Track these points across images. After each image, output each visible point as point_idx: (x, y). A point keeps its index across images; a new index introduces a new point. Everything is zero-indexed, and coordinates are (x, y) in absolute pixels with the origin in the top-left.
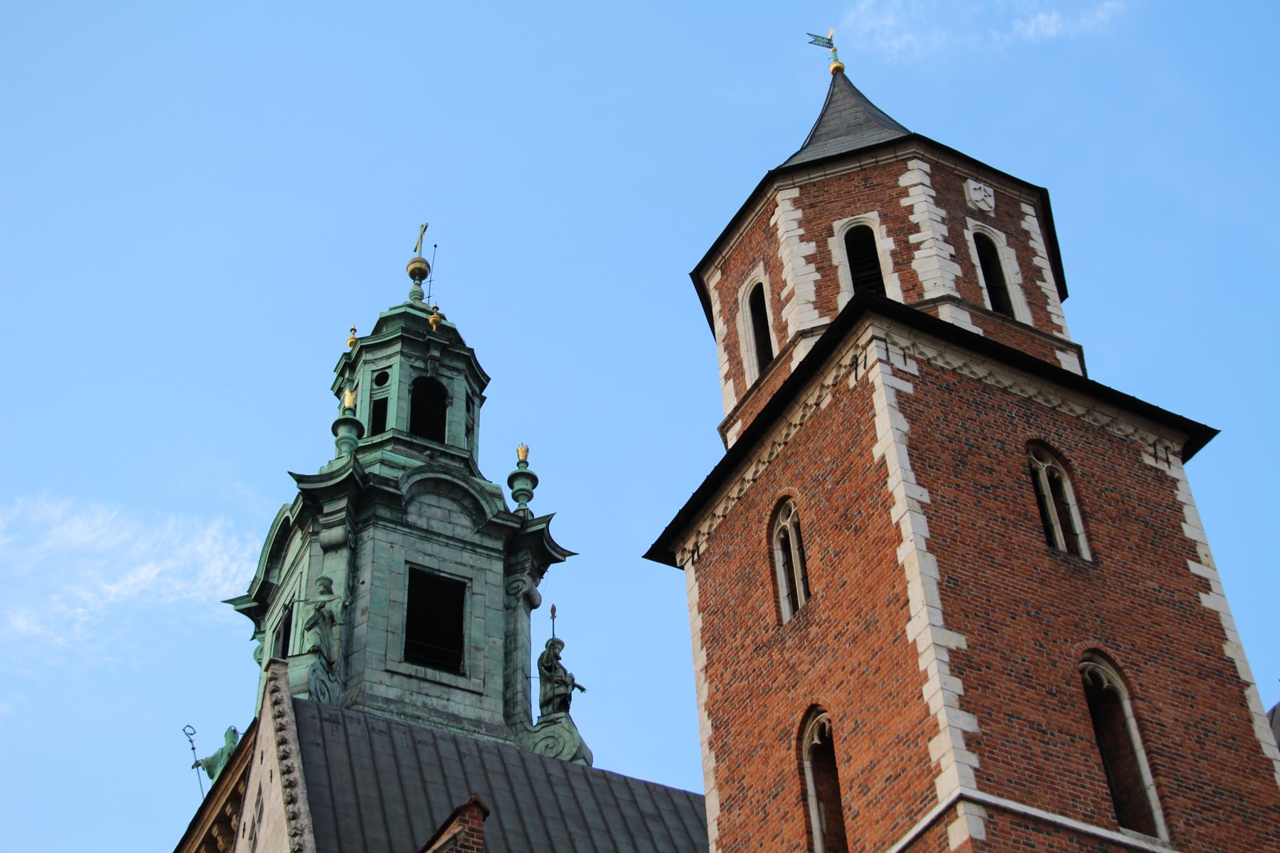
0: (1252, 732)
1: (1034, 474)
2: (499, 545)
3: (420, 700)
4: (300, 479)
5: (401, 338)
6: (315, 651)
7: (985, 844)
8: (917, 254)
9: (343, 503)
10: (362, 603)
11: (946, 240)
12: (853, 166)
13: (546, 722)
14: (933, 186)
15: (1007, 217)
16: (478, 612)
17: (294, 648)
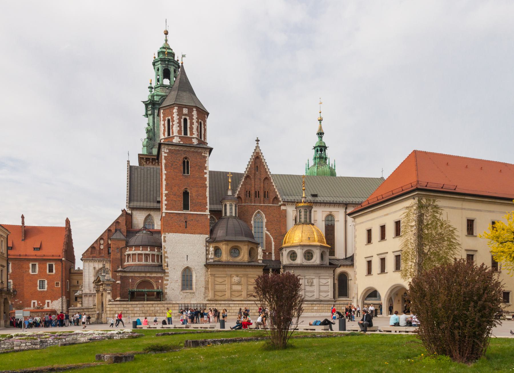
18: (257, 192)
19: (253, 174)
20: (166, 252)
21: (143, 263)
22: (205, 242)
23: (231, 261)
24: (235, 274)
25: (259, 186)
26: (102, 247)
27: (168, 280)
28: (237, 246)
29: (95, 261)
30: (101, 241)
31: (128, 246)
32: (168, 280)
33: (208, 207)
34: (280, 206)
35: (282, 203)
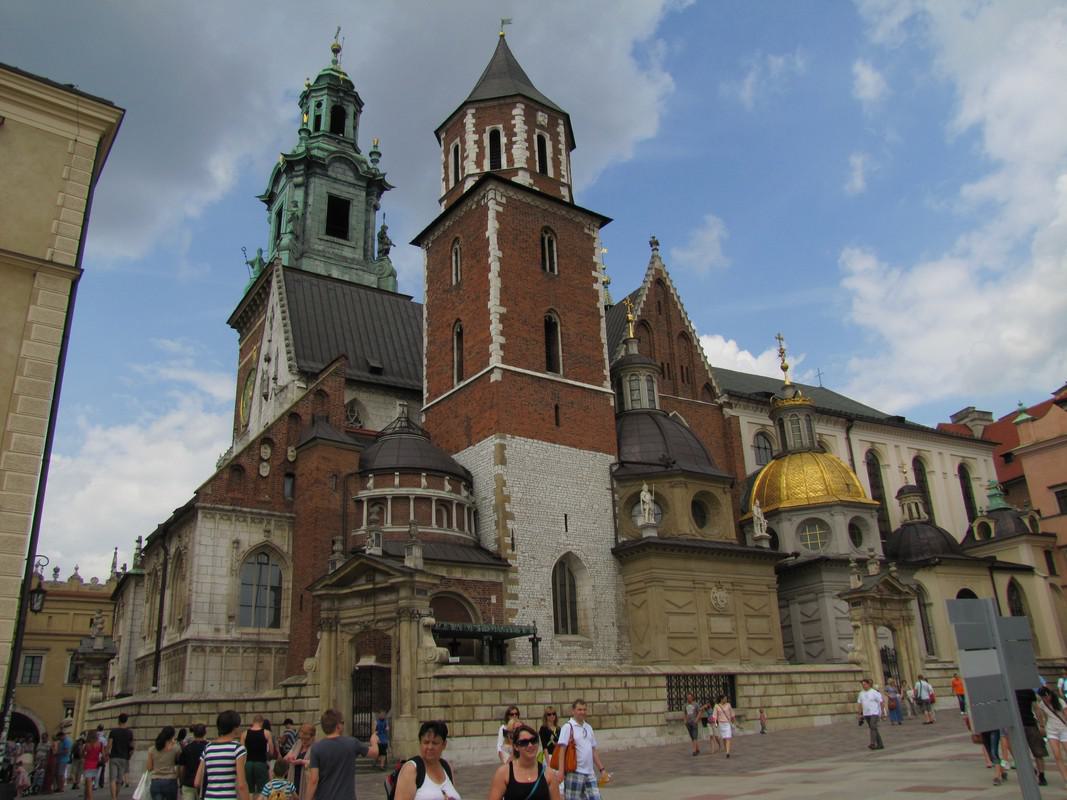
0: (599, 334)
1: (543, 239)
2: (364, 184)
3: (331, 250)
4: (285, 156)
5: (328, 88)
6: (291, 232)
7: (501, 382)
8: (515, 146)
9: (302, 167)
10: (309, 209)
11: (526, 141)
12: (495, 103)
13: (379, 257)
14: (524, 116)
15: (553, 124)
16: (355, 213)
17: (283, 231)
18: (666, 366)
19: (654, 320)
20: (507, 499)
21: (434, 529)
22: (608, 478)
23: (700, 538)
24: (715, 579)
25: (668, 351)
26: (265, 470)
27: (515, 597)
28: (708, 493)
29: (242, 517)
30: (262, 450)
31: (372, 471)
32: (515, 597)
33: (607, 372)
34: (721, 407)
35: (723, 399)
